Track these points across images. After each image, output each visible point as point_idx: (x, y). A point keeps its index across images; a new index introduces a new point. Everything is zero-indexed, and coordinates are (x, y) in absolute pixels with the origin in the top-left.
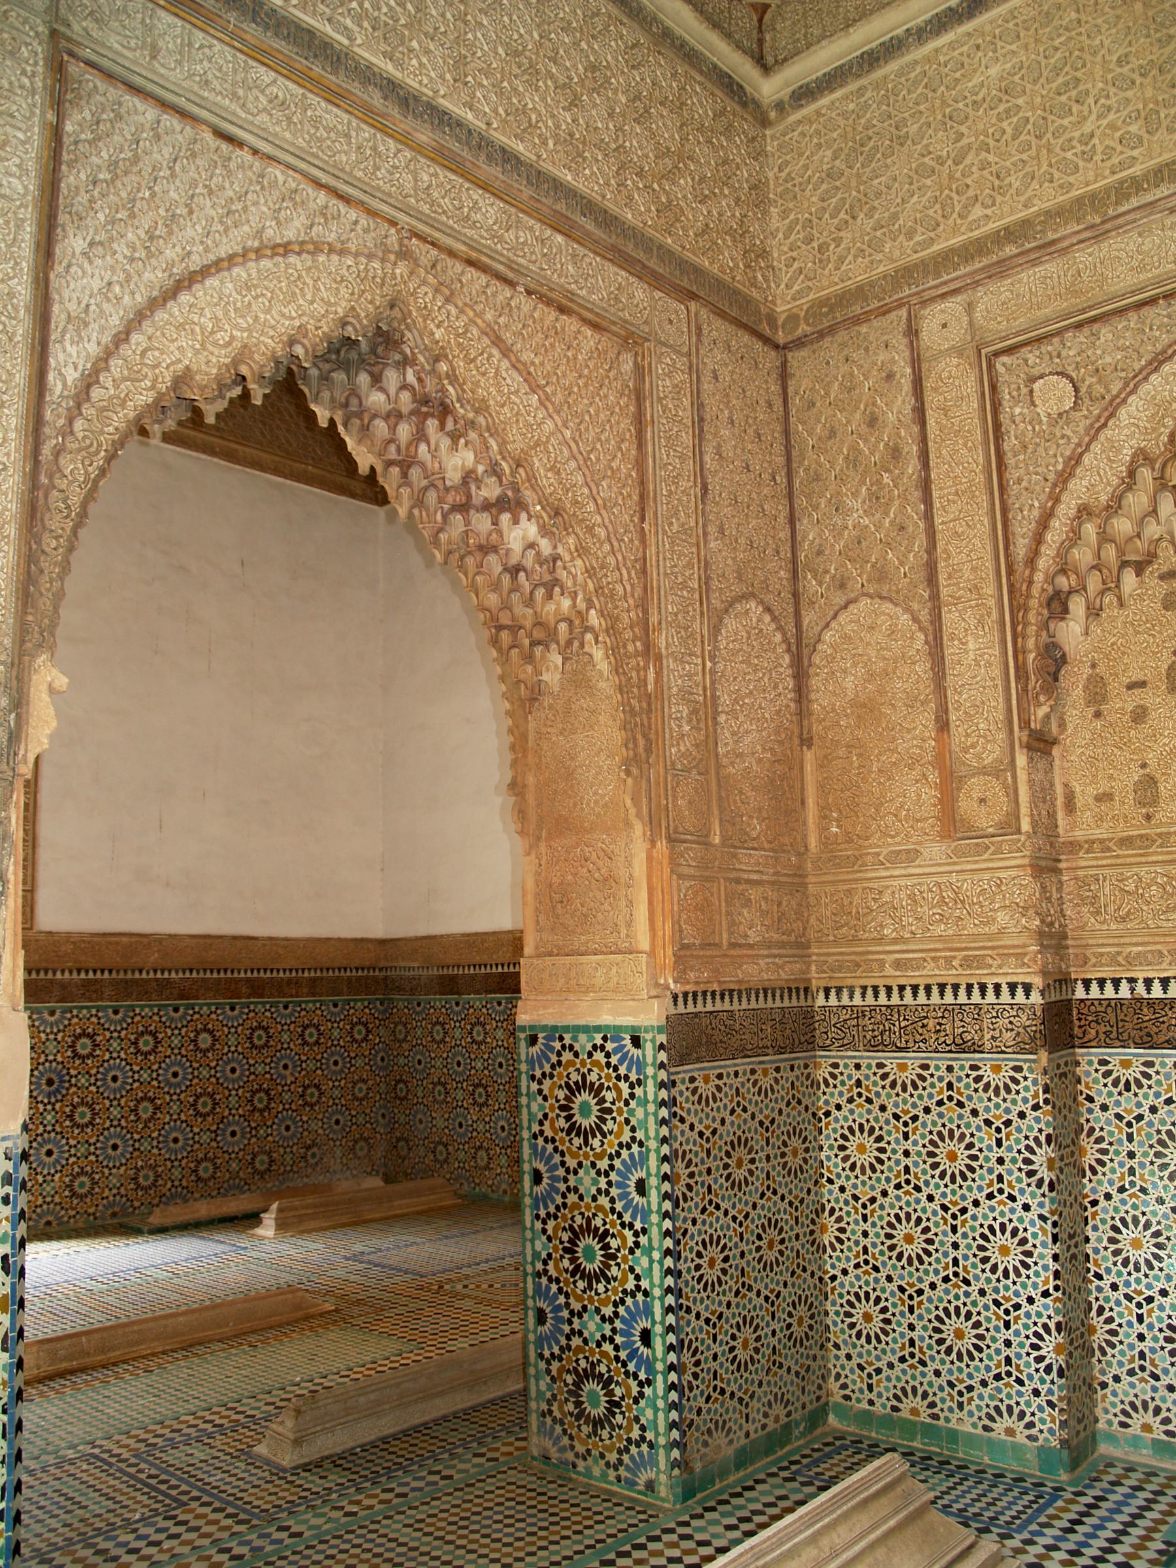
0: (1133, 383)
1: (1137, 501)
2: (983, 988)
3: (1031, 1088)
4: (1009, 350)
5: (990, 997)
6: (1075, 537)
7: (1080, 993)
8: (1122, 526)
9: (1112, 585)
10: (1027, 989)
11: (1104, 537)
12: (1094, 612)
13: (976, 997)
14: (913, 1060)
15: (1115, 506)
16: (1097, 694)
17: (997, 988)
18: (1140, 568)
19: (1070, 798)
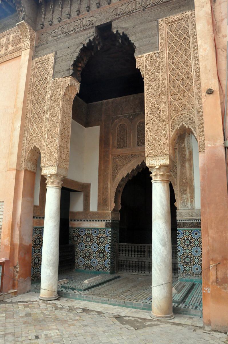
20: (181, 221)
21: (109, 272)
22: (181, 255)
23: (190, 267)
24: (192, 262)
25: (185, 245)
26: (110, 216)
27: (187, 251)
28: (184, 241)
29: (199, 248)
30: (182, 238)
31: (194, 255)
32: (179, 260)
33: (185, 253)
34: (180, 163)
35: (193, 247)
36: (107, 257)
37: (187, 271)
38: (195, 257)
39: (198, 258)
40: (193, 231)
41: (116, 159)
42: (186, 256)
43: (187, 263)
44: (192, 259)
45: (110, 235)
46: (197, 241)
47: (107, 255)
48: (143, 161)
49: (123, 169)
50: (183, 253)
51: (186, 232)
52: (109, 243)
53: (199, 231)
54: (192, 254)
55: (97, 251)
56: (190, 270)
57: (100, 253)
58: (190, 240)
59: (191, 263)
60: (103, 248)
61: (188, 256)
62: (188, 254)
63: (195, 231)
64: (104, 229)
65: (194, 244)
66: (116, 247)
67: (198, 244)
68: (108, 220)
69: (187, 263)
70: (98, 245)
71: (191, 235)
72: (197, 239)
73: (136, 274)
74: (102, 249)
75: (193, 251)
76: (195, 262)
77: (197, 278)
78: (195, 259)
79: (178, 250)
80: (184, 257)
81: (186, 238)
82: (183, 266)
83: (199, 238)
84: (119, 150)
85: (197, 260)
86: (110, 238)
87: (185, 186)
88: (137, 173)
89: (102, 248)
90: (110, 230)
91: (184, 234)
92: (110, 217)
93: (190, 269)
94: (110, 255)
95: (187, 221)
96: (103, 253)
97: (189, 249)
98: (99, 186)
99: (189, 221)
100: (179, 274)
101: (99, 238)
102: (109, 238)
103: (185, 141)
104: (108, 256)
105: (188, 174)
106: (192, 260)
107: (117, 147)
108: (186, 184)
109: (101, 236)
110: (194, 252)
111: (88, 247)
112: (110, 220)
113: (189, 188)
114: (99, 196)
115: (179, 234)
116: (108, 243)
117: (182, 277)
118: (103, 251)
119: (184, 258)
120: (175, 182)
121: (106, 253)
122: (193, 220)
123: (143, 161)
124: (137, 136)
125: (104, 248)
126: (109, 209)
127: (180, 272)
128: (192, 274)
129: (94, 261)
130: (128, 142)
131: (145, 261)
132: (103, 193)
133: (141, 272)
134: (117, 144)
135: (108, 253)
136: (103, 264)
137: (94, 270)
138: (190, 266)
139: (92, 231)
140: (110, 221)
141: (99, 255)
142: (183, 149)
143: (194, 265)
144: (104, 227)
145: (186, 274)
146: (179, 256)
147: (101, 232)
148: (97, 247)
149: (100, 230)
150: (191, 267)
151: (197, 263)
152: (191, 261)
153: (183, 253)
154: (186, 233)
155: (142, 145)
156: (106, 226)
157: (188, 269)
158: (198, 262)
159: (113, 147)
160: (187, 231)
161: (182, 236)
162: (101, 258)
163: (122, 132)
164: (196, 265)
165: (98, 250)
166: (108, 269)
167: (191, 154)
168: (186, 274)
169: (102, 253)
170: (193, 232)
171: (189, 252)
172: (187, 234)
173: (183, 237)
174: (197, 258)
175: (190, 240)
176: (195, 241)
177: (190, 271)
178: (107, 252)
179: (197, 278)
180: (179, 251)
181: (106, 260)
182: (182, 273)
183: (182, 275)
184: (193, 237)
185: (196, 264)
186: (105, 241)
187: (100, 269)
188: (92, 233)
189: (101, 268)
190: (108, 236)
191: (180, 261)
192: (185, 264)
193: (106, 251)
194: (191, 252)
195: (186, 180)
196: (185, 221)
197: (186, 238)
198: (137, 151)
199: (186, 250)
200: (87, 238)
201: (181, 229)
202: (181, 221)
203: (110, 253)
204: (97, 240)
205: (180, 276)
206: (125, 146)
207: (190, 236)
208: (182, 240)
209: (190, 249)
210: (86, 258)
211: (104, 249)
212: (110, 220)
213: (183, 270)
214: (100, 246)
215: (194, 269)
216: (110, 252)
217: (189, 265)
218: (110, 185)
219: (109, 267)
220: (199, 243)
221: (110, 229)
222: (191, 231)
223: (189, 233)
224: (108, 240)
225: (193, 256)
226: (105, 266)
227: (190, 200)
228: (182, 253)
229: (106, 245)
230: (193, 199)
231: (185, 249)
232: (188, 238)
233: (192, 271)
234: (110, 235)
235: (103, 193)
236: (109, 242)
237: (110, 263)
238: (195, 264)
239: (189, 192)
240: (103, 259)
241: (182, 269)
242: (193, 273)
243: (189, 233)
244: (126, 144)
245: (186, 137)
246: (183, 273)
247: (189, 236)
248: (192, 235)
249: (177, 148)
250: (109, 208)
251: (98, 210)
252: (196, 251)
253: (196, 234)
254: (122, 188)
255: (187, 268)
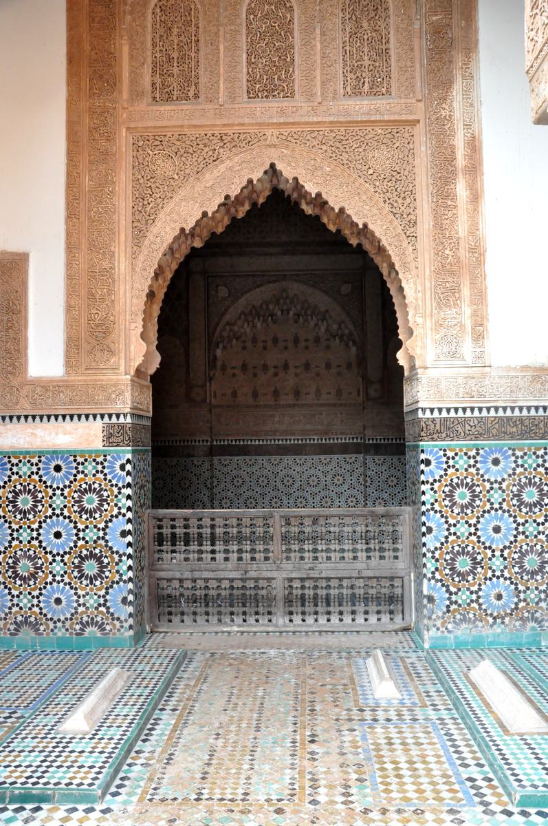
0: (242, 294)
1: (239, 323)
2: (195, 441)
3: (207, 465)
4: (213, 276)
5: (197, 443)
6: (224, 329)
7: (215, 443)
8: (236, 328)
9: (230, 341)
10: (207, 441)
11: (231, 330)
12: (225, 348)
13: (193, 443)
14: (175, 460)
15: (234, 324)
16: (224, 368)
17: (199, 441)
18: (237, 339)
19: (215, 393)
20: (436, 412)
21: (130, 636)
22: (438, 545)
23: (472, 589)
24: (479, 570)
25: (451, 507)
26: (128, 395)
27: (462, 530)
28: (450, 491)
29: (506, 515)
30: (440, 481)
31: (487, 544)
32: (431, 565)
33: (452, 538)
34: (431, 181)
35: (484, 512)
36: (118, 572)
37: (460, 605)
38: (493, 551)
39: (502, 556)
40: (485, 452)
41: (149, 152)
42: (457, 548)
43: (459, 574)
44: (479, 558)
45: (129, 479)
46: (500, 488)
47: (117, 564)
48: (272, 166)
49: (182, 193)
50: (447, 537)
51: (456, 454)
52: (124, 515)
53: (506, 451)
54: (479, 542)
55: (68, 550)
56: (472, 601)
57: (83, 559)
58: (473, 485)
59: (475, 574)
60: (99, 538)
61: (463, 548)
62: (463, 542)
63: (490, 449)
64: (98, 453)
65: (489, 500)
66: (145, 526)
67: (504, 500)
68: (118, 416)
69: (459, 574)
70: (76, 523)
71: (474, 466)
72: (500, 483)
73: (236, 629)
74: (95, 542)
75: (485, 530)
76: (490, 568)
77: (498, 629)
78: (490, 559)
79: (424, 529)
80: (447, 553)
81: (455, 481)
82: (444, 589)
83: (506, 476)
84: (166, 108)
85: (498, 563)
86: (129, 491)
87: (452, 273)
88: (227, 221)
89: (91, 534)
90: (129, 456)
91: (447, 462)
92: (129, 402)
93: (474, 597)
94: (130, 562)
95: (460, 413)
96: (99, 560)
97: (467, 522)
98: (69, 264)
99: (468, 413)
100: (430, 618)
101: (76, 495)
102: (123, 491)
103: (454, 94)
104: (125, 568)
105: (462, 229)
106: (479, 563)
107: (154, 98)
108: (455, 268)
109: (84, 486)
110: (486, 533)
111: (25, 536)
112: (125, 416)
113: (467, 283)
114: (69, 308)
115: (428, 463)
116: (120, 513)
117: (443, 632)
118: (97, 551)
119: (448, 557)
120: (410, 258)
121: (113, 559)
122: (485, 411)
123: (272, 166)
124: (245, 56)
125: (101, 534)
126: (122, 368)
127: (433, 613)
128: (480, 615)
129: (56, 596)
130: (203, 80)
131: (269, 575)
132: (91, 295)
133: (257, 621)
134: (153, 84)
135: (120, 556)
136: (100, 605)
137: (60, 634)
138: (473, 585)
139: (41, 465)
140: (129, 420)
141: (79, 567)
142: (446, 127)
143: (488, 582)
144: (98, 444)
145: (458, 617)
146: (429, 550)
147: (86, 468)
148: (69, 535)
149: (80, 460)
150: (475, 588)
151: (498, 573)
152: (476, 568)
153: (447, 537)
154: (457, 458)
155: (267, 97)
156: (108, 438)
157: (464, 597)
158: (502, 571)
159: (136, 95)
160: (461, 450)
161: (442, 473)
162: (92, 580)
163: (175, 31)
164: (494, 579)
165: (72, 544)
166: (126, 625)
167: (474, 146)
168: (458, 617)
169: (92, 556)
170: (482, 456)
171: (467, 534)
172: (461, 462)
173: (446, 475)
174: (498, 553)
175: (471, 487)
176: (492, 488)
177: (475, 605)
178: (117, 552)
179: (499, 630)
180: (430, 530)
181: (115, 586)
182: (440, 614)
183: (443, 624)
184: (482, 476)
185: (494, 576)
186: (106, 506)
187: (84, 625)
188: (41, 472)
189: (92, 622)
190: (120, 485)
191: (433, 569)
192: (453, 580)
193: (111, 548)
194: (475, 534)
195: (456, 247)
196: (452, 414)
197: (455, 481)
198: (246, 121)
199: (458, 526)
200: (17, 494)
201: (436, 446)
202: (436, 412)
203: (129, 556)
204: (69, 502)
205: (434, 626)
206: (191, 94)
207: (472, 470)
208: (440, 487)
209: (473, 521)
210: (19, 582)
211: (103, 538)
212: (125, 416)
213: (448, 603)
214: (81, 526)
215: (488, 596)
216: (130, 551)
217: (468, 581)
218: (122, 259)
219: (130, 615)
220: (508, 495)
221: (128, 452)
222: (478, 449)
223: (469, 457)
224: (119, 501)
225: (485, 548)
226: (111, 610)
227: (473, 329)
228: (443, 540)
229: (111, 521)
230: (482, 325)
231: (452, 521)
232: (466, 478)
233: (480, 605)
234: (129, 479)
235: (91, 295)
236: (123, 511)
237: (131, 598)
238: (490, 579)
239: (467, 299)
240: (98, 583)
241: (442, 599)
242: (485, 610)
243: (469, 457)
244: (196, 84)
245: (459, 78)
246: (444, 613)
247: (466, 470)
248: (478, 465)
249: (418, 121)
250: (122, 362)
251: (67, 373)
252: (497, 530)
253: (496, 462)
254: (160, 281)
255: (460, 593)
